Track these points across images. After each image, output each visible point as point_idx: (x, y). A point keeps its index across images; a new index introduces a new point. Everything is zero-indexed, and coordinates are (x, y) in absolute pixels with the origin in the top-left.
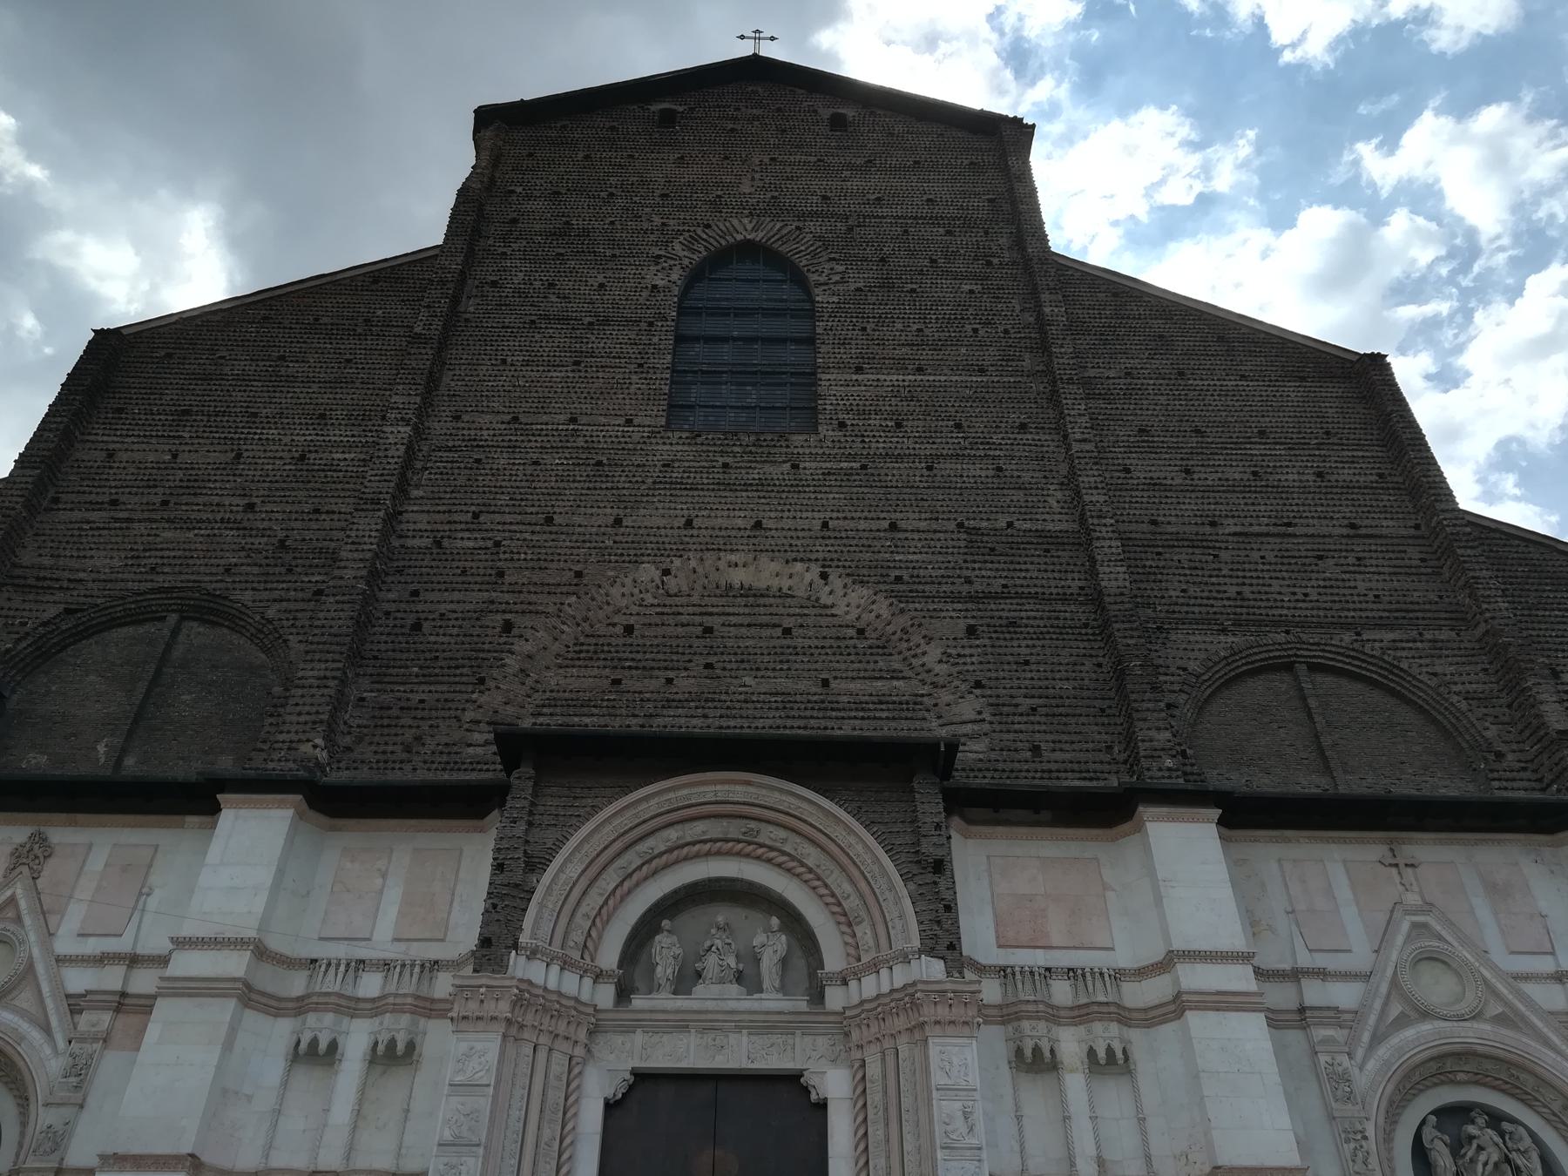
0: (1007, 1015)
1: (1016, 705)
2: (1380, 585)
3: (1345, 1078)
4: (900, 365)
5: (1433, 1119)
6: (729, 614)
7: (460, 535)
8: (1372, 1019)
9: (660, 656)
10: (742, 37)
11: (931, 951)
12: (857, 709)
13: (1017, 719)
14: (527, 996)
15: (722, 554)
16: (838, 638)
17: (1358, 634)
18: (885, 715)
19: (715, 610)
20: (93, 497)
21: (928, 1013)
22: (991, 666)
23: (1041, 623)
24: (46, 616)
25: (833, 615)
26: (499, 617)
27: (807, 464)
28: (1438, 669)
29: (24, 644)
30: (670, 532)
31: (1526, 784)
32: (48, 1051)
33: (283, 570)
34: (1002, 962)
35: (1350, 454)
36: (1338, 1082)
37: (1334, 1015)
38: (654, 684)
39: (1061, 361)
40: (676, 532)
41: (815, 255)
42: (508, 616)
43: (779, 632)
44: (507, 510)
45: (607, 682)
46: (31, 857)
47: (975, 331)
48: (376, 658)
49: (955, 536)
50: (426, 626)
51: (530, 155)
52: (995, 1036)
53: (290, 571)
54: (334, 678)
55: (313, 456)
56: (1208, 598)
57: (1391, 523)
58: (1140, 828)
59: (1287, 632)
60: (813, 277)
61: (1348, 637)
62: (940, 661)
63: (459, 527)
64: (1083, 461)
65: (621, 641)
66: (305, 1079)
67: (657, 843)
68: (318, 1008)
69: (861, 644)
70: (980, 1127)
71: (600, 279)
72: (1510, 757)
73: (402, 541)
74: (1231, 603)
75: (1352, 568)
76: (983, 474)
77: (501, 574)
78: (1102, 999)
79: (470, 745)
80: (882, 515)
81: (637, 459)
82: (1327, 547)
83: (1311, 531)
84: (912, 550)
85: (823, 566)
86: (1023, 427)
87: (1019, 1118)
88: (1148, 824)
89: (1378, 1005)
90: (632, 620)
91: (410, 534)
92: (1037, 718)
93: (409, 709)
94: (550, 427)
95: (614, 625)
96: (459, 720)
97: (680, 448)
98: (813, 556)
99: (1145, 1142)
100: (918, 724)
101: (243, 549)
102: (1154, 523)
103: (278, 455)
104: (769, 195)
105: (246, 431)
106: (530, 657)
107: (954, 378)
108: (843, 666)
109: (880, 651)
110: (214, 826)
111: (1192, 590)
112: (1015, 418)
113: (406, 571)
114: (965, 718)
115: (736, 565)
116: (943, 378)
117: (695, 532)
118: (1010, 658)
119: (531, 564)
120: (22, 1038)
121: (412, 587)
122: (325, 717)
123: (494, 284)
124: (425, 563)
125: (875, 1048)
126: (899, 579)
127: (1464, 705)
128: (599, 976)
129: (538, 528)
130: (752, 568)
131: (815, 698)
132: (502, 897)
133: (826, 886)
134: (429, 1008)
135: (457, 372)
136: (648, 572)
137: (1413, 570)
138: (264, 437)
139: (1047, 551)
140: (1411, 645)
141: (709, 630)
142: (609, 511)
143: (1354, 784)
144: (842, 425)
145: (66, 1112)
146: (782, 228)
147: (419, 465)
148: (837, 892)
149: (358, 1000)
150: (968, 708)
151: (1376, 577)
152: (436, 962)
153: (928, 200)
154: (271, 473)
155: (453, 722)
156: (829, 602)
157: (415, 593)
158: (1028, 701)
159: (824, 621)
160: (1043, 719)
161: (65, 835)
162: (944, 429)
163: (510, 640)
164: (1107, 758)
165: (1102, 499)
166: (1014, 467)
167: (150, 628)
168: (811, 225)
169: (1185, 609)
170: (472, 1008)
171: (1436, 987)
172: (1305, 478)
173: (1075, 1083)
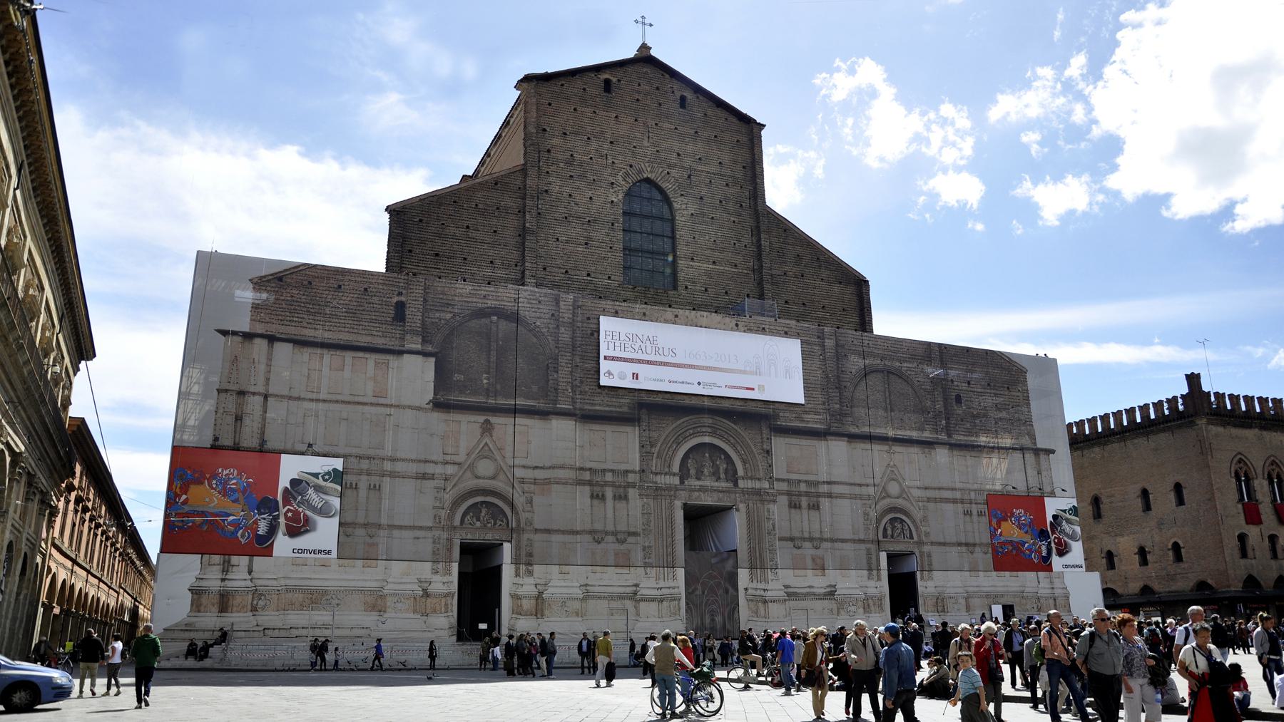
132: (645, 456)
145: (531, 514)
168: (673, 171)
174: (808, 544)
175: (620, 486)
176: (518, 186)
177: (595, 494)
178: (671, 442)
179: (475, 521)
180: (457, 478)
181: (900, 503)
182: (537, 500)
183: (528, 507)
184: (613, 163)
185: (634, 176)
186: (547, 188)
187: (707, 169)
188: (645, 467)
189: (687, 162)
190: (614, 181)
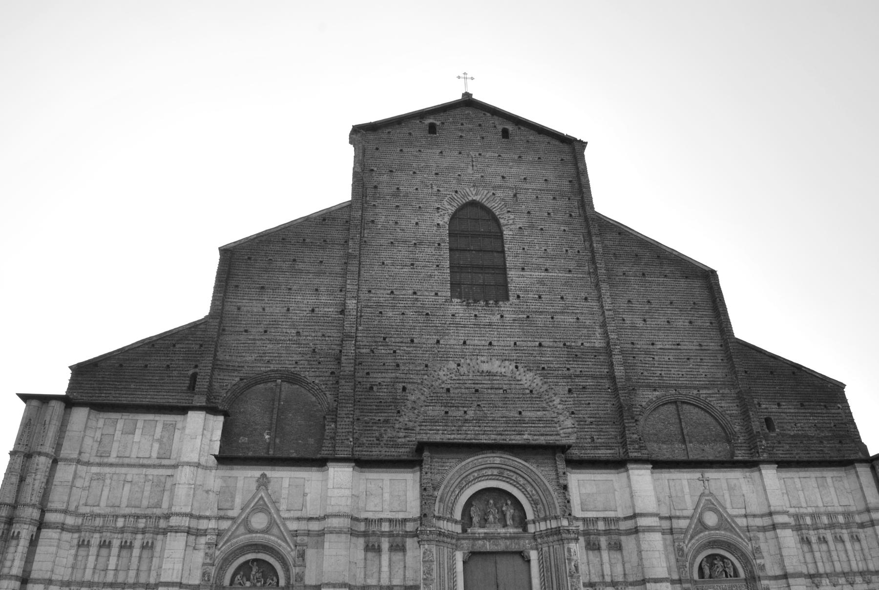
0: (586, 533)
1: (586, 421)
2: (707, 371)
3: (682, 550)
4: (538, 268)
5: (705, 559)
6: (484, 384)
7: (380, 348)
9: (461, 402)
12: (532, 423)
13: (586, 427)
15: (479, 357)
17: (698, 391)
18: (542, 425)
19: (480, 382)
20: (237, 329)
21: (564, 535)
22: (577, 405)
23: (593, 387)
24: (234, 382)
25: (521, 384)
27: (507, 316)
28: (723, 405)
29: (229, 394)
30: (458, 347)
31: (745, 448)
32: (289, 549)
33: (317, 363)
34: (583, 516)
35: (701, 313)
38: (461, 413)
39: (601, 271)
42: (404, 384)
43: (501, 391)
44: (395, 336)
45: (444, 412)
46: (263, 482)
48: (359, 402)
49: (563, 349)
50: (375, 388)
51: (377, 149)
53: (319, 363)
54: (351, 414)
55: (317, 309)
56: (650, 376)
57: (713, 344)
58: (627, 470)
59: (676, 390)
60: (502, 221)
61: (695, 392)
62: (560, 404)
63: (380, 344)
64: (609, 319)
66: (370, 555)
71: (417, 221)
72: (741, 438)
73: (359, 350)
74: (657, 378)
75: (698, 364)
76: (572, 320)
77: (398, 365)
78: (613, 528)
79: (399, 438)
80: (536, 340)
82: (690, 354)
83: (685, 347)
84: (548, 355)
85: (516, 363)
86: (586, 299)
88: (630, 471)
89: (693, 526)
90: (449, 386)
91: (362, 347)
92: (593, 426)
93: (375, 423)
94: (406, 296)
95: (443, 388)
97: (457, 307)
98: (512, 358)
99: (624, 570)
101: (300, 353)
102: (633, 343)
103: (304, 309)
104: (480, 176)
105: (289, 297)
106: (414, 402)
107: (560, 275)
108: (526, 406)
109: (539, 399)
110: (328, 475)
111: (645, 373)
112: (583, 295)
113: (364, 364)
114: (569, 426)
115: (484, 362)
116: (556, 274)
117: (468, 347)
118: (583, 402)
119: (408, 361)
120: (280, 546)
121: (368, 371)
122: (351, 430)
123: (373, 222)
124: (369, 360)
125: (546, 545)
126: (543, 368)
127: (729, 419)
128: (456, 522)
129: (409, 345)
130: (490, 363)
131: (517, 419)
132: (427, 499)
133: (526, 491)
135: (366, 268)
137: (718, 364)
138: (296, 300)
139: (595, 356)
140: (715, 395)
141: (477, 391)
142: (434, 337)
143: (692, 456)
144: (518, 297)
145: (302, 568)
146: (487, 194)
148: (530, 493)
149: (383, 532)
150: (569, 423)
151: (706, 367)
152: (406, 519)
153: (546, 180)
154: (303, 318)
155: (392, 429)
156: (519, 379)
157: (368, 374)
158: (590, 419)
159: (518, 387)
160: (594, 426)
162: (557, 300)
163: (406, 394)
165: (616, 337)
166: (583, 318)
167: (271, 385)
168: (500, 193)
169: (642, 381)
172: (685, 324)
173: (605, 554)
175: (398, 535)
176: (345, 220)
177: (370, 545)
178: (454, 487)
179: (245, 579)
180: (230, 533)
181: (722, 534)
182: (310, 553)
183: (299, 562)
184: (438, 190)
186: (372, 219)
187: (533, 186)
188: (426, 511)
189: (511, 182)
190: (439, 206)
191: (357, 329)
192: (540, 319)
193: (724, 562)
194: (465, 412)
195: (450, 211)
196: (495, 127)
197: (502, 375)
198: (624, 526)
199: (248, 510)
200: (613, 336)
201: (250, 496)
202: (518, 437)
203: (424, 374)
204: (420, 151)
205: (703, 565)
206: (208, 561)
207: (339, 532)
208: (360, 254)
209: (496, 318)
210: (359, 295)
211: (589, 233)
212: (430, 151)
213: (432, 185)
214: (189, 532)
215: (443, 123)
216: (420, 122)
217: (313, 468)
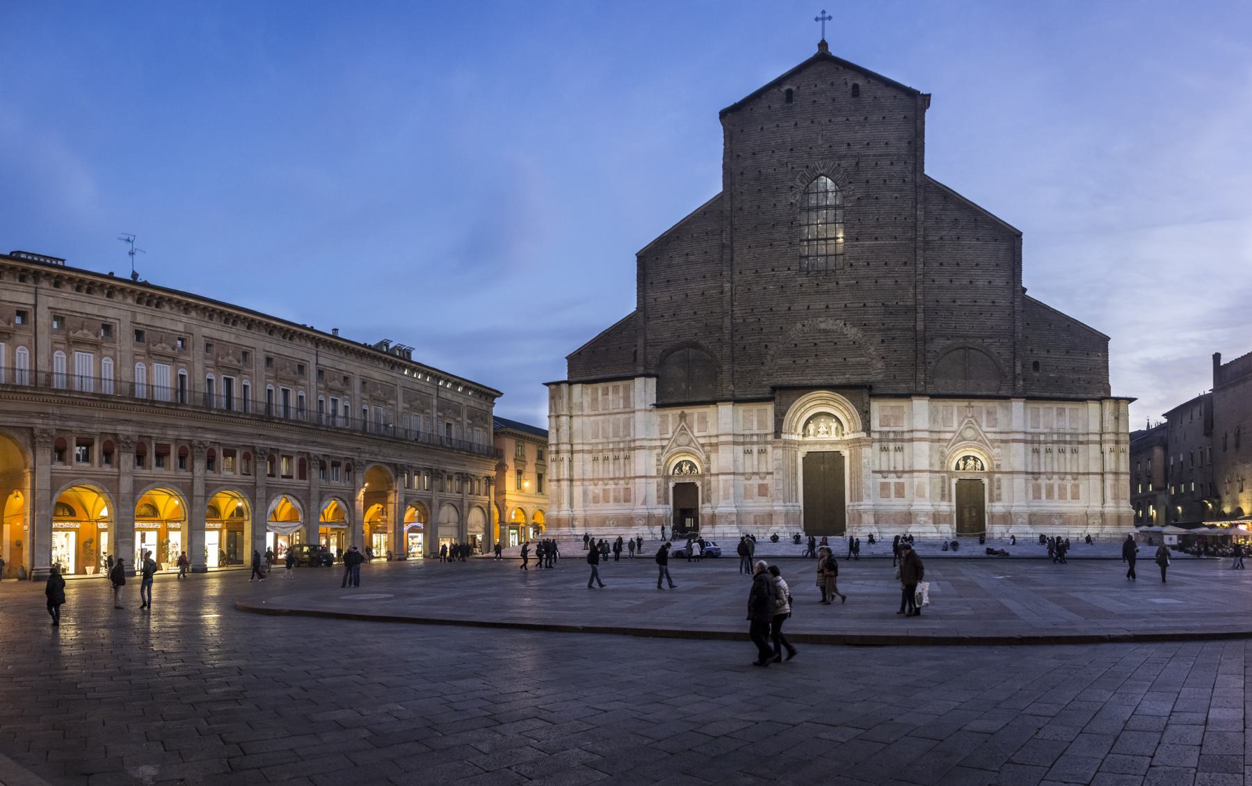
0: (880, 440)
8: (953, 441)
10: (817, 19)
11: (863, 430)
14: (786, 442)
16: (848, 345)
26: (764, 344)
36: (942, 453)
37: (945, 440)
39: (919, 239)
40: (805, 311)
41: (844, 180)
45: (791, 362)
46: (683, 416)
47: (895, 218)
50: (747, 348)
52: (876, 446)
53: (710, 333)
65: (793, 349)
66: (747, 456)
67: (808, 406)
68: (747, 444)
69: (854, 346)
70: (871, 464)
71: (774, 202)
76: (891, 283)
77: (762, 330)
81: (793, 284)
86: (905, 263)
87: (880, 460)
88: (914, 401)
90: (796, 342)
96: (759, 374)
98: (844, 317)
99: (903, 464)
100: (867, 370)
107: (887, 242)
111: (944, 326)
112: (904, 259)
116: (883, 242)
117: (810, 311)
123: (741, 208)
126: (865, 325)
134: (767, 443)
136: (799, 326)
141: (815, 344)
142: (787, 305)
144: (851, 265)
147: (734, 292)
150: (880, 365)
153: (887, 143)
157: (742, 338)
161: (687, 411)
164: (910, 378)
168: (844, 163)
170: (776, 445)
171: (969, 433)
174: (893, 475)
182: (713, 456)
184: (793, 168)
185: (809, 176)
191: (732, 305)
192: (866, 284)
193: (975, 461)
194: (807, 360)
195: (801, 188)
196: (846, 83)
197: (834, 331)
198: (907, 436)
199: (676, 434)
200: (920, 297)
201: (677, 425)
202: (841, 377)
203: (779, 335)
204: (778, 126)
205: (959, 462)
206: (658, 463)
207: (726, 443)
208: (732, 242)
209: (832, 286)
210: (733, 276)
211: (916, 198)
212: (786, 124)
213: (787, 163)
214: (642, 448)
215: (798, 88)
216: (779, 90)
217: (711, 406)
